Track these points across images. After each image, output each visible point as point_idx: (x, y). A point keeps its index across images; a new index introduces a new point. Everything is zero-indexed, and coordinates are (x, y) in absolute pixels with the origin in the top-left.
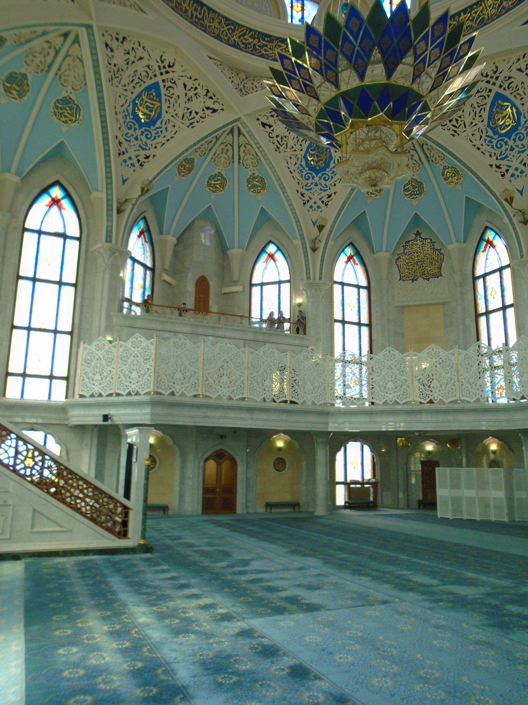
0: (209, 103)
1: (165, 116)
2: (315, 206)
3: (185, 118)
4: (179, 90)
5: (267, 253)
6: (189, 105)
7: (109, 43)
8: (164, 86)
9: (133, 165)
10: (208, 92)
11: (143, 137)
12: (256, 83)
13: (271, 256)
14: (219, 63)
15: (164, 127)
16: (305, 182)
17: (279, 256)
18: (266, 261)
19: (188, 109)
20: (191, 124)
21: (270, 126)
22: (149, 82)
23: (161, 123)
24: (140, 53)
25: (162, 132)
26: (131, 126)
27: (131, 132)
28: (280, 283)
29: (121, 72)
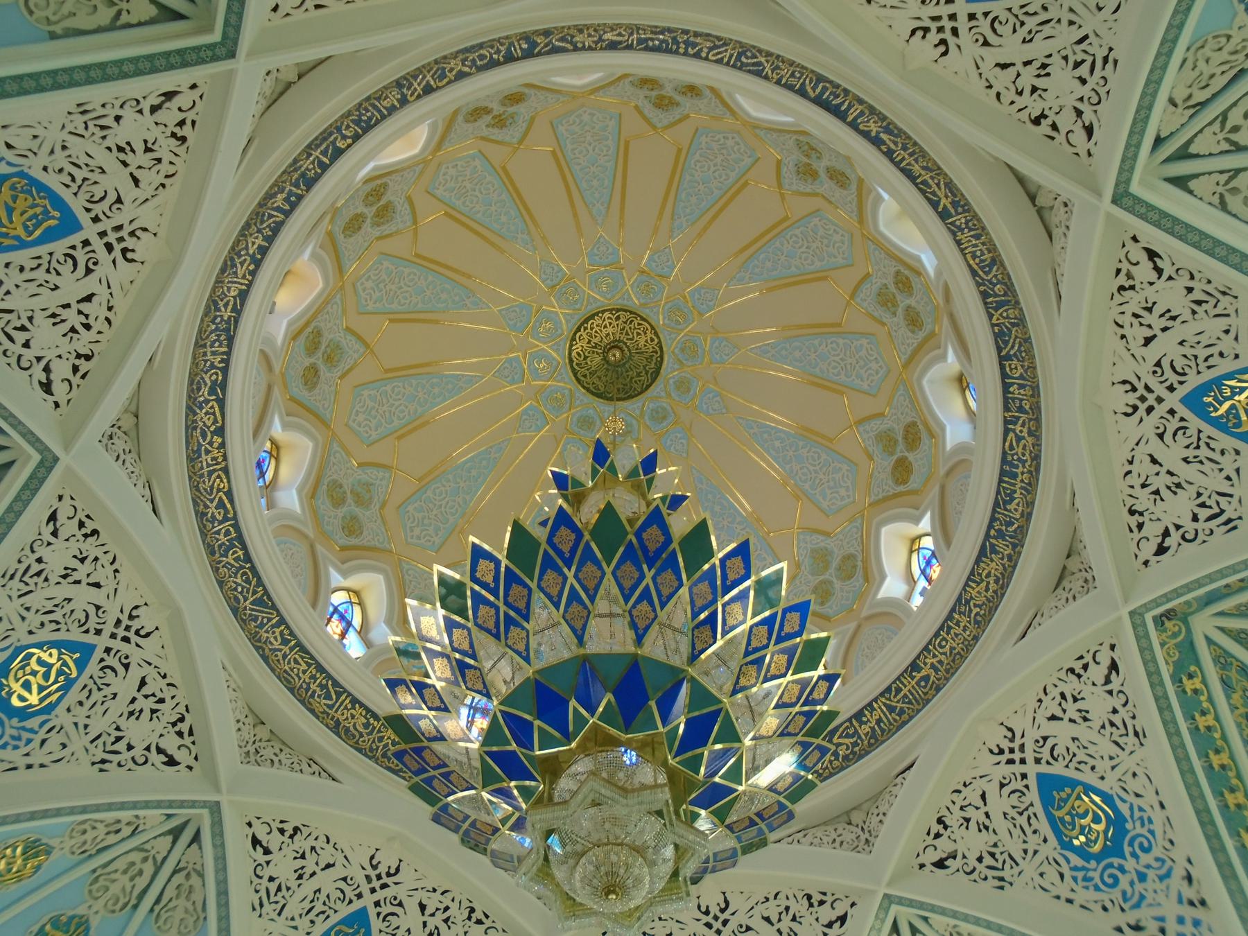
0: (171, 743)
1: (60, 717)
3: (100, 741)
6: (122, 723)
7: (61, 517)
8: (102, 660)
10: (182, 720)
12: (282, 756)
14: (233, 686)
15: (42, 734)
19: (118, 729)
20: (103, 761)
21: (267, 851)
23: (42, 724)
24: (103, 574)
25: (29, 741)
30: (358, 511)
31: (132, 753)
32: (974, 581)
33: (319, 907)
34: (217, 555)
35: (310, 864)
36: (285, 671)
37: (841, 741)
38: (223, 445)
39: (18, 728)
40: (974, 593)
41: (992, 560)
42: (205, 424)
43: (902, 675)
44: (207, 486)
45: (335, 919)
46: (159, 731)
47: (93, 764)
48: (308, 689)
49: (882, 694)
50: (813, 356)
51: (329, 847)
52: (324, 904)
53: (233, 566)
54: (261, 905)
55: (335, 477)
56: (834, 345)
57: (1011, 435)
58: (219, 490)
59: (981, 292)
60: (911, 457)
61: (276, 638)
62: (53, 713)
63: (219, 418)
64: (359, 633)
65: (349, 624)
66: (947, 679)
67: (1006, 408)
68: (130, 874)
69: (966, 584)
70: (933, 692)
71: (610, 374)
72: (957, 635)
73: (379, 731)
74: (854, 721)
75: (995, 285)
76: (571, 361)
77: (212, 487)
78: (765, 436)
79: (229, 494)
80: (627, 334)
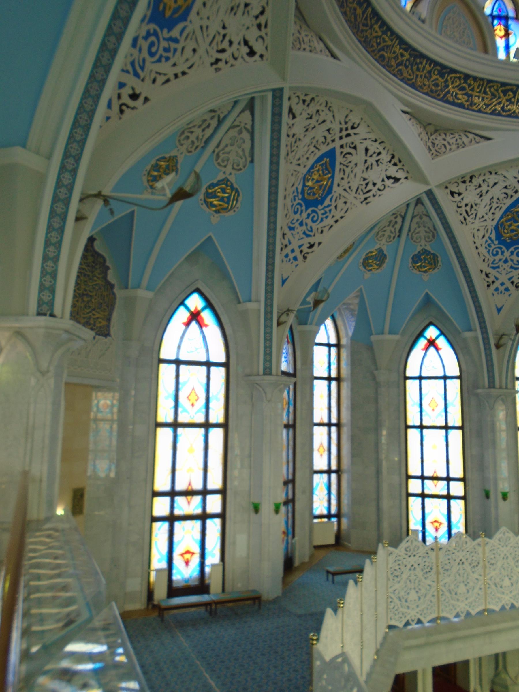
0: (393, 171)
1: (337, 190)
2: (502, 288)
3: (359, 190)
4: (359, 157)
5: (426, 338)
6: (365, 175)
8: (341, 153)
9: (295, 258)
11: (309, 221)
13: (431, 343)
16: (491, 260)
17: (442, 342)
18: (426, 349)
19: (365, 179)
20: (366, 199)
22: (324, 149)
23: (331, 200)
25: (330, 211)
26: (298, 209)
27: (297, 216)
28: (445, 378)
29: (298, 143)
31: (377, 186)
33: (495, 205)
35: (484, 188)
39: (323, 209)
45: (504, 208)
46: (384, 170)
47: (362, 202)
51: (493, 176)
52: (497, 203)
54: (465, 219)
62: (333, 192)
68: (392, 225)
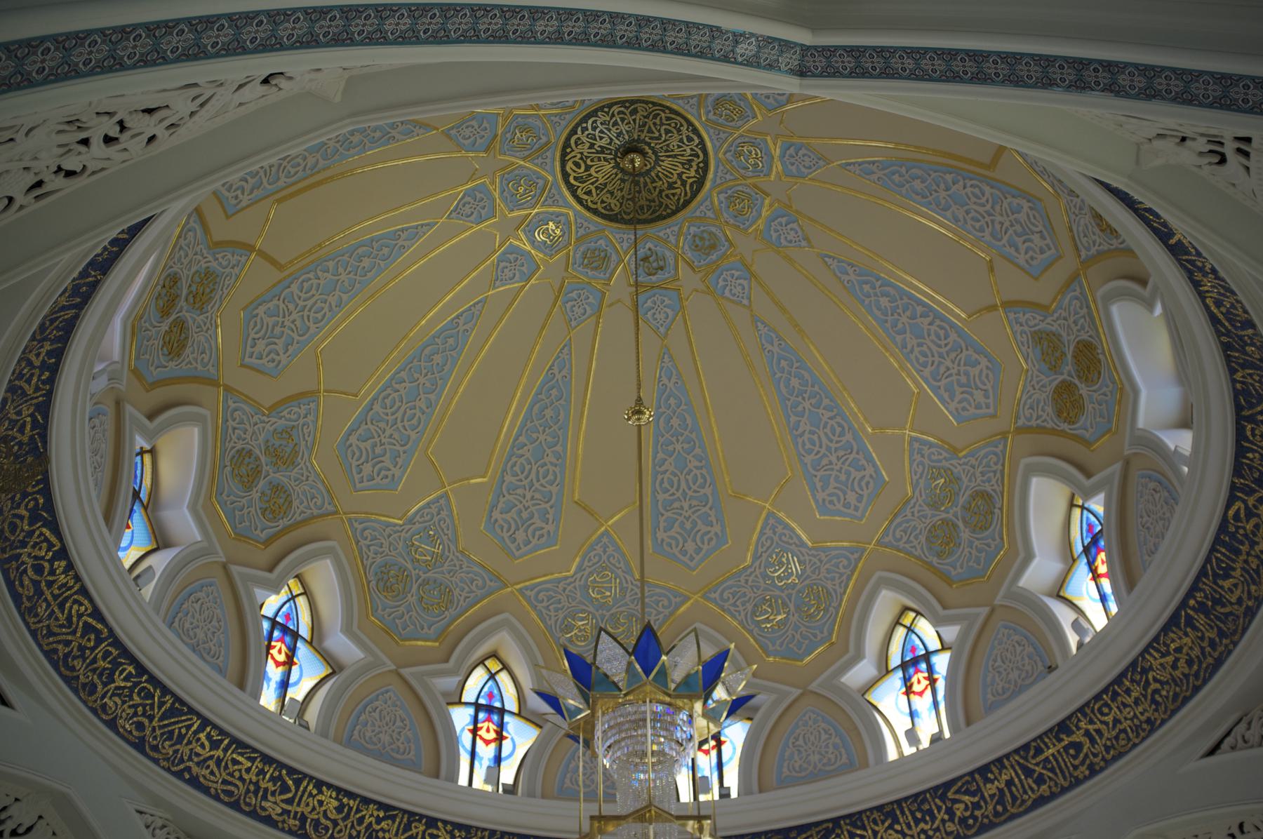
14: (160, 823)
30: (280, 477)
32: (1158, 650)
34: (100, 687)
36: (225, 782)
37: (957, 797)
38: (70, 566)
40: (1155, 664)
41: (1186, 634)
42: (36, 558)
43: (1045, 733)
44: (62, 621)
48: (258, 788)
49: (1016, 751)
50: (943, 194)
53: (124, 687)
55: (239, 447)
56: (977, 191)
57: (1238, 504)
58: (80, 616)
59: (1222, 343)
60: (1083, 390)
61: (203, 746)
63: (53, 539)
64: (310, 643)
65: (296, 635)
66: (1108, 763)
67: (1237, 470)
69: (1146, 650)
70: (1084, 770)
71: (627, 185)
72: (1125, 705)
73: (358, 811)
74: (977, 776)
75: (1246, 344)
76: (565, 176)
77: (69, 618)
78: (866, 288)
79: (97, 614)
80: (650, 131)
